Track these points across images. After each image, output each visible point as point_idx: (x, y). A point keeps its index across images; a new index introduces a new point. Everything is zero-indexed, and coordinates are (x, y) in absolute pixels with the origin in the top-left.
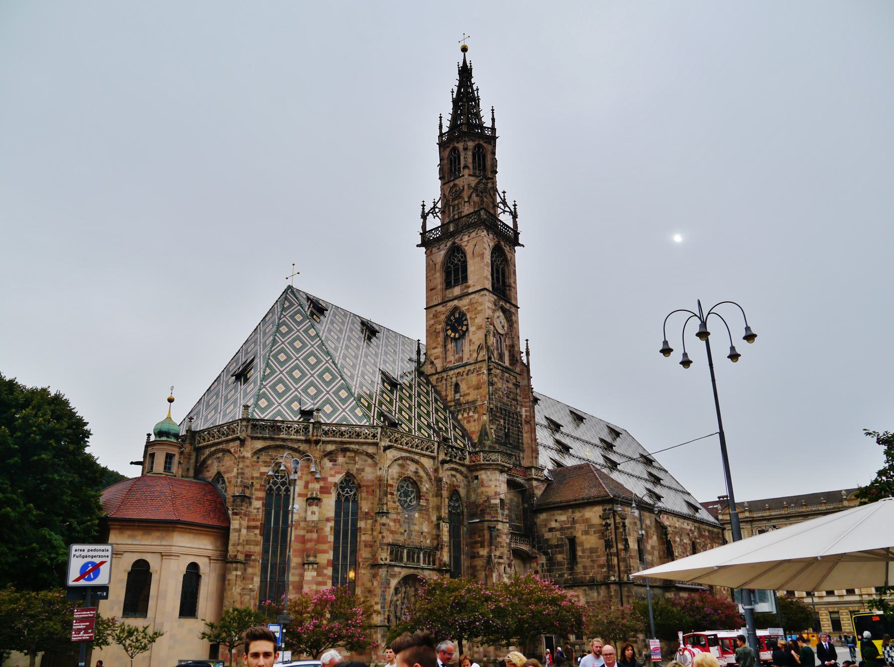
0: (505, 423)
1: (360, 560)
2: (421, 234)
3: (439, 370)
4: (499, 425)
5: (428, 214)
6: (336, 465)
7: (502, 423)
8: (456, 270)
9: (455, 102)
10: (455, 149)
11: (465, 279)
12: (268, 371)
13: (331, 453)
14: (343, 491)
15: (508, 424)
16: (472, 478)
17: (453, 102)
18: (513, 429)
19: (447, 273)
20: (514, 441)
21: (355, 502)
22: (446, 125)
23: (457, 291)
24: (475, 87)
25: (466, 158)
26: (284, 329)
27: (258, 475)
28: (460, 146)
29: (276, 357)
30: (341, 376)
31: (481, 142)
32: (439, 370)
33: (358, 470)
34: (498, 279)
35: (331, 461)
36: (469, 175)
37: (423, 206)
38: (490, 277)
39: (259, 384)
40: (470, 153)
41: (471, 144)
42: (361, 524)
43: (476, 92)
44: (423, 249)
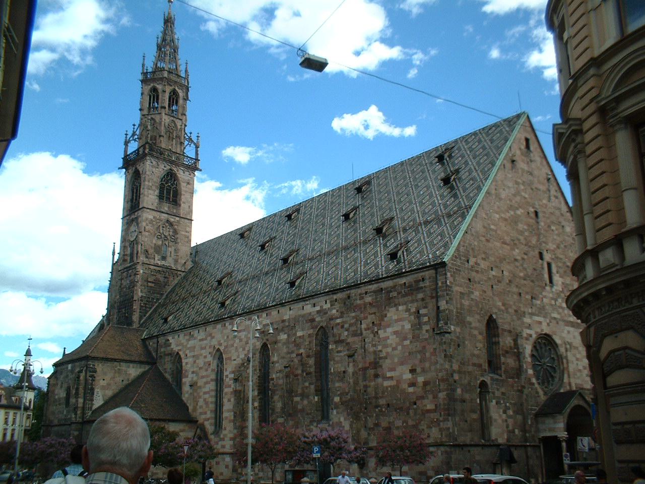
2: (122, 158)
5: (129, 141)
9: (159, 48)
10: (155, 90)
17: (158, 44)
22: (150, 67)
24: (176, 37)
25: (165, 99)
28: (160, 87)
31: (177, 89)
36: (165, 114)
37: (126, 134)
40: (167, 95)
41: (168, 89)
43: (176, 41)
44: (124, 170)
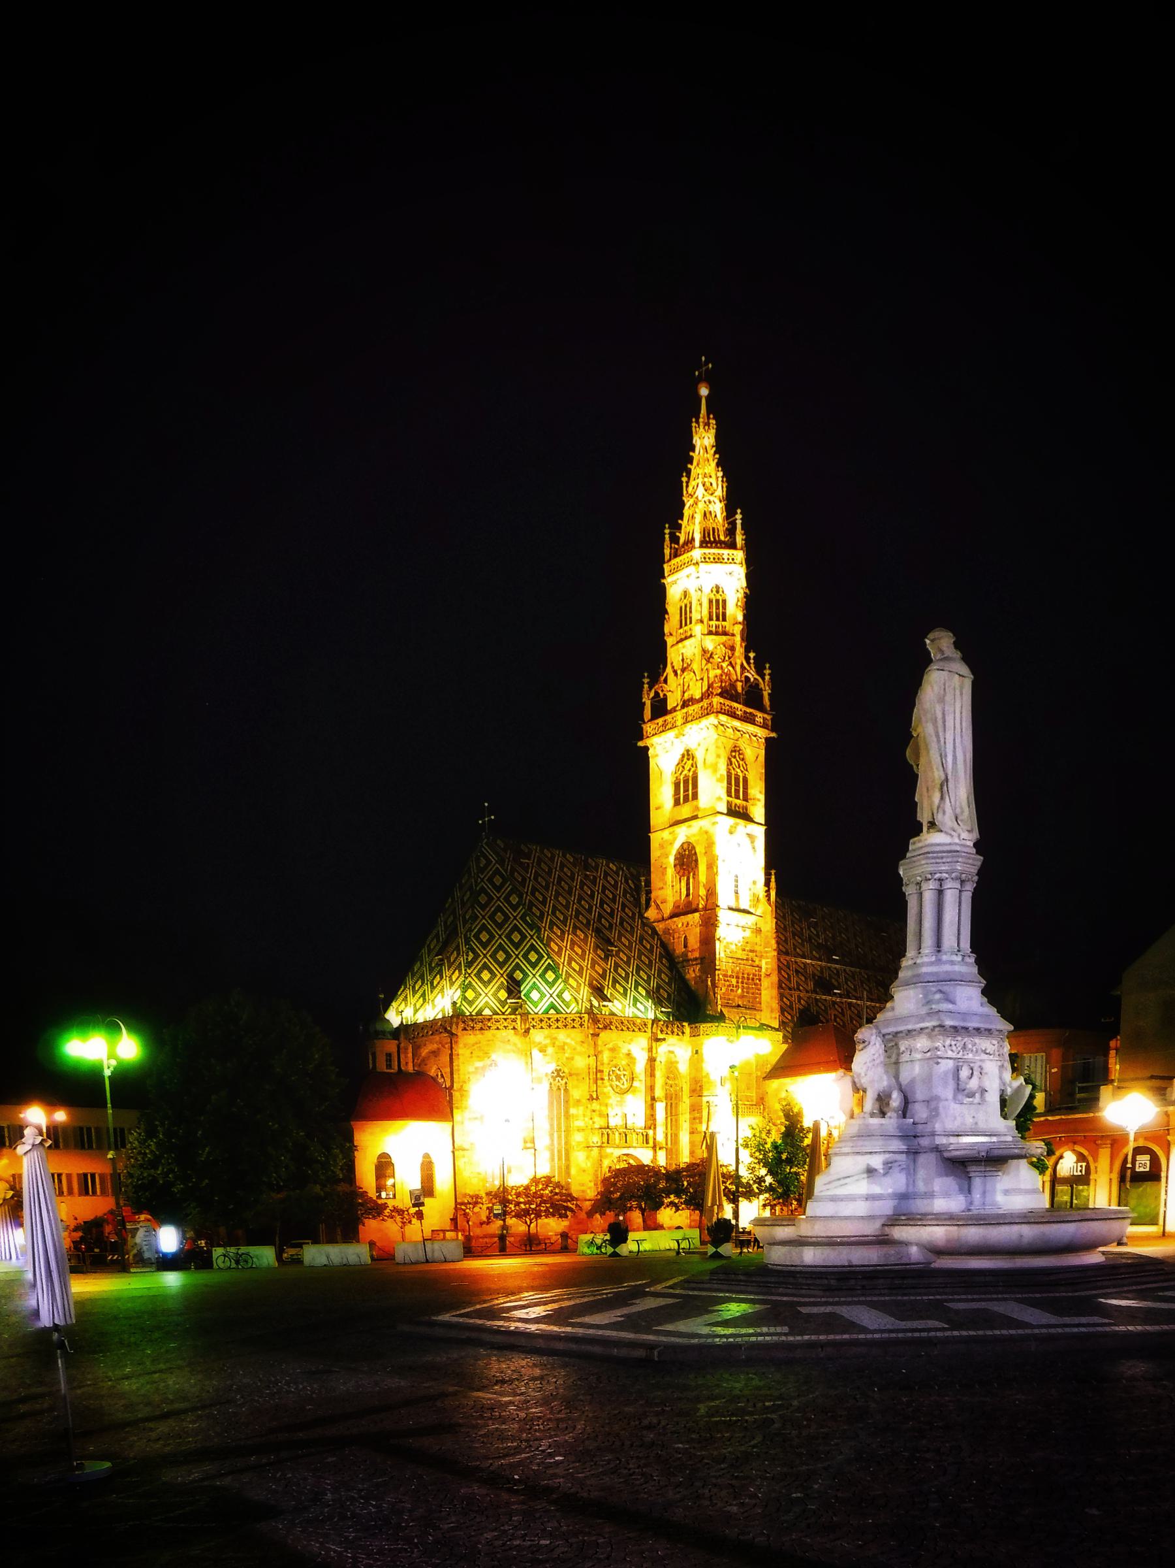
0: (738, 982)
1: (573, 1143)
3: (666, 916)
4: (729, 986)
6: (545, 1055)
7: (735, 984)
8: (686, 782)
11: (695, 796)
12: (471, 956)
13: (540, 1043)
14: (555, 1080)
15: (742, 983)
16: (692, 1052)
18: (748, 988)
19: (677, 785)
20: (749, 1001)
21: (566, 1090)
23: (685, 811)
26: (483, 899)
27: (474, 1070)
29: (477, 937)
30: (548, 954)
32: (666, 916)
33: (567, 1058)
34: (737, 791)
35: (541, 1051)
38: (725, 798)
39: (463, 972)
42: (572, 1111)
